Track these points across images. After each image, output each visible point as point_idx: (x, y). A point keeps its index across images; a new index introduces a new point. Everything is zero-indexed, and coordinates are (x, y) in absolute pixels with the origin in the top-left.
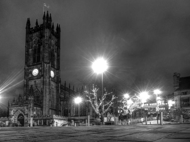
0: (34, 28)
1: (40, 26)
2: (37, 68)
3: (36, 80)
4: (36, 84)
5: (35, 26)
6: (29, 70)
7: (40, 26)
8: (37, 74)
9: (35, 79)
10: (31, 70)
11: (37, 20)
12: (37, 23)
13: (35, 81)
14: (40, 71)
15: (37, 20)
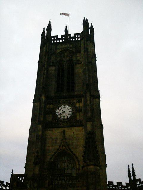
0: (60, 37)
1: (72, 35)
2: (69, 104)
3: (66, 129)
4: (65, 139)
5: (64, 34)
6: (48, 106)
7: (72, 35)
8: (69, 116)
9: (63, 127)
10: (51, 106)
11: (66, 26)
12: (66, 31)
13: (64, 132)
14: (76, 110)
15: (66, 26)
